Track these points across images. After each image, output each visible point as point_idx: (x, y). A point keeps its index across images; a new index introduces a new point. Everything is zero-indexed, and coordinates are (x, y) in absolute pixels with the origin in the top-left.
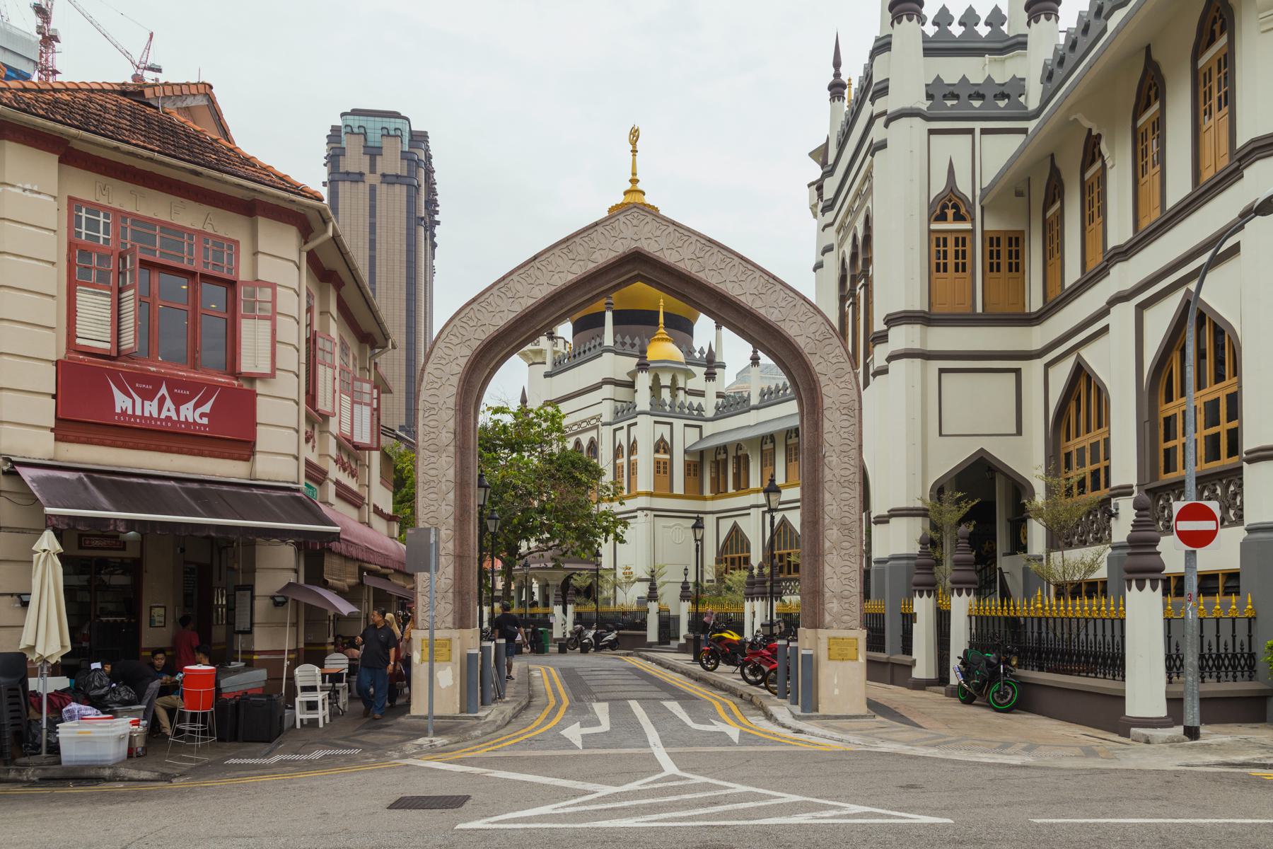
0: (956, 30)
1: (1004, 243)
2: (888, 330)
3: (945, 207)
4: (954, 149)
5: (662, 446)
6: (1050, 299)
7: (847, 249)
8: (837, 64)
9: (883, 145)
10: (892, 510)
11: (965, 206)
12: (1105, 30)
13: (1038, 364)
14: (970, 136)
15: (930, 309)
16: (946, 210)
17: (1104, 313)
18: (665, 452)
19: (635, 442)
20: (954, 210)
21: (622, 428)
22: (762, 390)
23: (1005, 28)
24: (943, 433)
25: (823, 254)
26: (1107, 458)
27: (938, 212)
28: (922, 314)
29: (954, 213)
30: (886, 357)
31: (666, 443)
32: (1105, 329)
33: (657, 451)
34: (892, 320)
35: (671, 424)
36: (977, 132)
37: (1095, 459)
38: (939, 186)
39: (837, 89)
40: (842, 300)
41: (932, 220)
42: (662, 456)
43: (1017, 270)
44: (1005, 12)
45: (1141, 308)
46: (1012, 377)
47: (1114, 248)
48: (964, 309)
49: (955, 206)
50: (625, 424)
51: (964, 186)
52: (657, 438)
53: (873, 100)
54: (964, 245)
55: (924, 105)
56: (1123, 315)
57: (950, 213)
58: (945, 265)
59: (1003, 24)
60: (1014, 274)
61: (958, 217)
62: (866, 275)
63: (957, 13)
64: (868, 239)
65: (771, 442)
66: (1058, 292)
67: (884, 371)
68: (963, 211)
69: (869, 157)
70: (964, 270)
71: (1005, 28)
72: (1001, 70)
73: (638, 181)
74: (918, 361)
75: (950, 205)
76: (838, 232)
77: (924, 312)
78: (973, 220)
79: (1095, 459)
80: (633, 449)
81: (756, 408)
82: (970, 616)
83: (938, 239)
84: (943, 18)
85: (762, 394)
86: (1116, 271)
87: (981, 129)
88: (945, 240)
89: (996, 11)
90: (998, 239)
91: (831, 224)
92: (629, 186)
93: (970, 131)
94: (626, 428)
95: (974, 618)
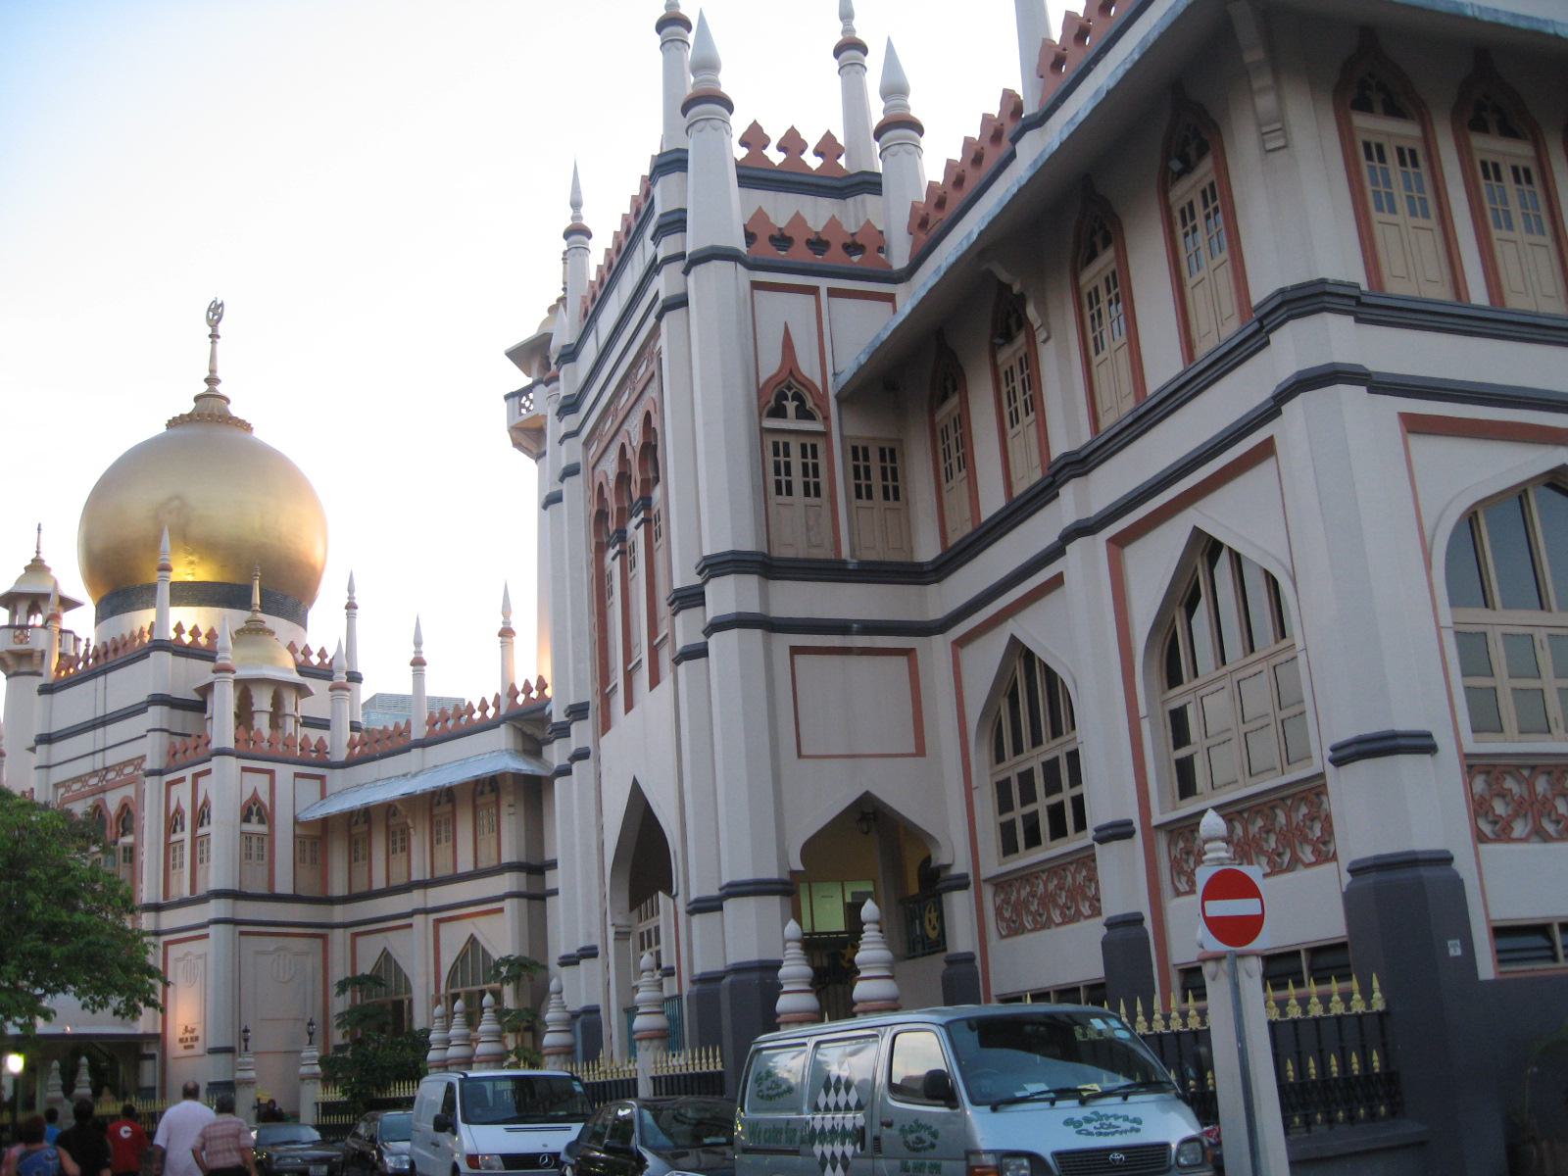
0: (776, 157)
1: (875, 456)
2: (705, 582)
3: (782, 396)
4: (786, 312)
5: (254, 810)
6: (951, 542)
7: (610, 467)
8: (576, 205)
9: (680, 302)
10: (729, 885)
11: (813, 398)
13: (941, 644)
15: (769, 550)
16: (784, 402)
17: (1056, 552)
18: (261, 821)
19: (206, 803)
20: (796, 403)
21: (182, 780)
22: (431, 715)
23: (842, 161)
25: (562, 480)
26: (1076, 779)
27: (773, 402)
28: (760, 559)
29: (797, 408)
32: (1058, 581)
33: (246, 819)
34: (716, 566)
35: (271, 772)
36: (823, 293)
37: (1053, 786)
38: (771, 364)
39: (577, 232)
40: (600, 549)
41: (765, 413)
44: (841, 140)
45: (1120, 542)
47: (1065, 455)
48: (824, 553)
49: (798, 397)
50: (188, 773)
51: (808, 365)
52: (247, 796)
54: (815, 455)
55: (739, 243)
56: (1085, 561)
57: (791, 406)
58: (789, 484)
59: (839, 156)
60: (891, 503)
61: (803, 413)
62: (646, 502)
63: (775, 133)
64: (650, 450)
65: (449, 801)
66: (968, 529)
67: (698, 652)
68: (810, 404)
69: (651, 320)
70: (818, 494)
71: (842, 161)
72: (853, 213)
74: (757, 634)
75: (790, 395)
76: (587, 444)
77: (763, 554)
78: (826, 418)
79: (1053, 786)
80: (201, 816)
81: (422, 744)
83: (776, 445)
84: (755, 138)
85: (432, 722)
86: (1068, 492)
87: (829, 289)
89: (829, 138)
90: (865, 450)
91: (575, 434)
92: (203, 388)
93: (813, 291)
94: (189, 779)
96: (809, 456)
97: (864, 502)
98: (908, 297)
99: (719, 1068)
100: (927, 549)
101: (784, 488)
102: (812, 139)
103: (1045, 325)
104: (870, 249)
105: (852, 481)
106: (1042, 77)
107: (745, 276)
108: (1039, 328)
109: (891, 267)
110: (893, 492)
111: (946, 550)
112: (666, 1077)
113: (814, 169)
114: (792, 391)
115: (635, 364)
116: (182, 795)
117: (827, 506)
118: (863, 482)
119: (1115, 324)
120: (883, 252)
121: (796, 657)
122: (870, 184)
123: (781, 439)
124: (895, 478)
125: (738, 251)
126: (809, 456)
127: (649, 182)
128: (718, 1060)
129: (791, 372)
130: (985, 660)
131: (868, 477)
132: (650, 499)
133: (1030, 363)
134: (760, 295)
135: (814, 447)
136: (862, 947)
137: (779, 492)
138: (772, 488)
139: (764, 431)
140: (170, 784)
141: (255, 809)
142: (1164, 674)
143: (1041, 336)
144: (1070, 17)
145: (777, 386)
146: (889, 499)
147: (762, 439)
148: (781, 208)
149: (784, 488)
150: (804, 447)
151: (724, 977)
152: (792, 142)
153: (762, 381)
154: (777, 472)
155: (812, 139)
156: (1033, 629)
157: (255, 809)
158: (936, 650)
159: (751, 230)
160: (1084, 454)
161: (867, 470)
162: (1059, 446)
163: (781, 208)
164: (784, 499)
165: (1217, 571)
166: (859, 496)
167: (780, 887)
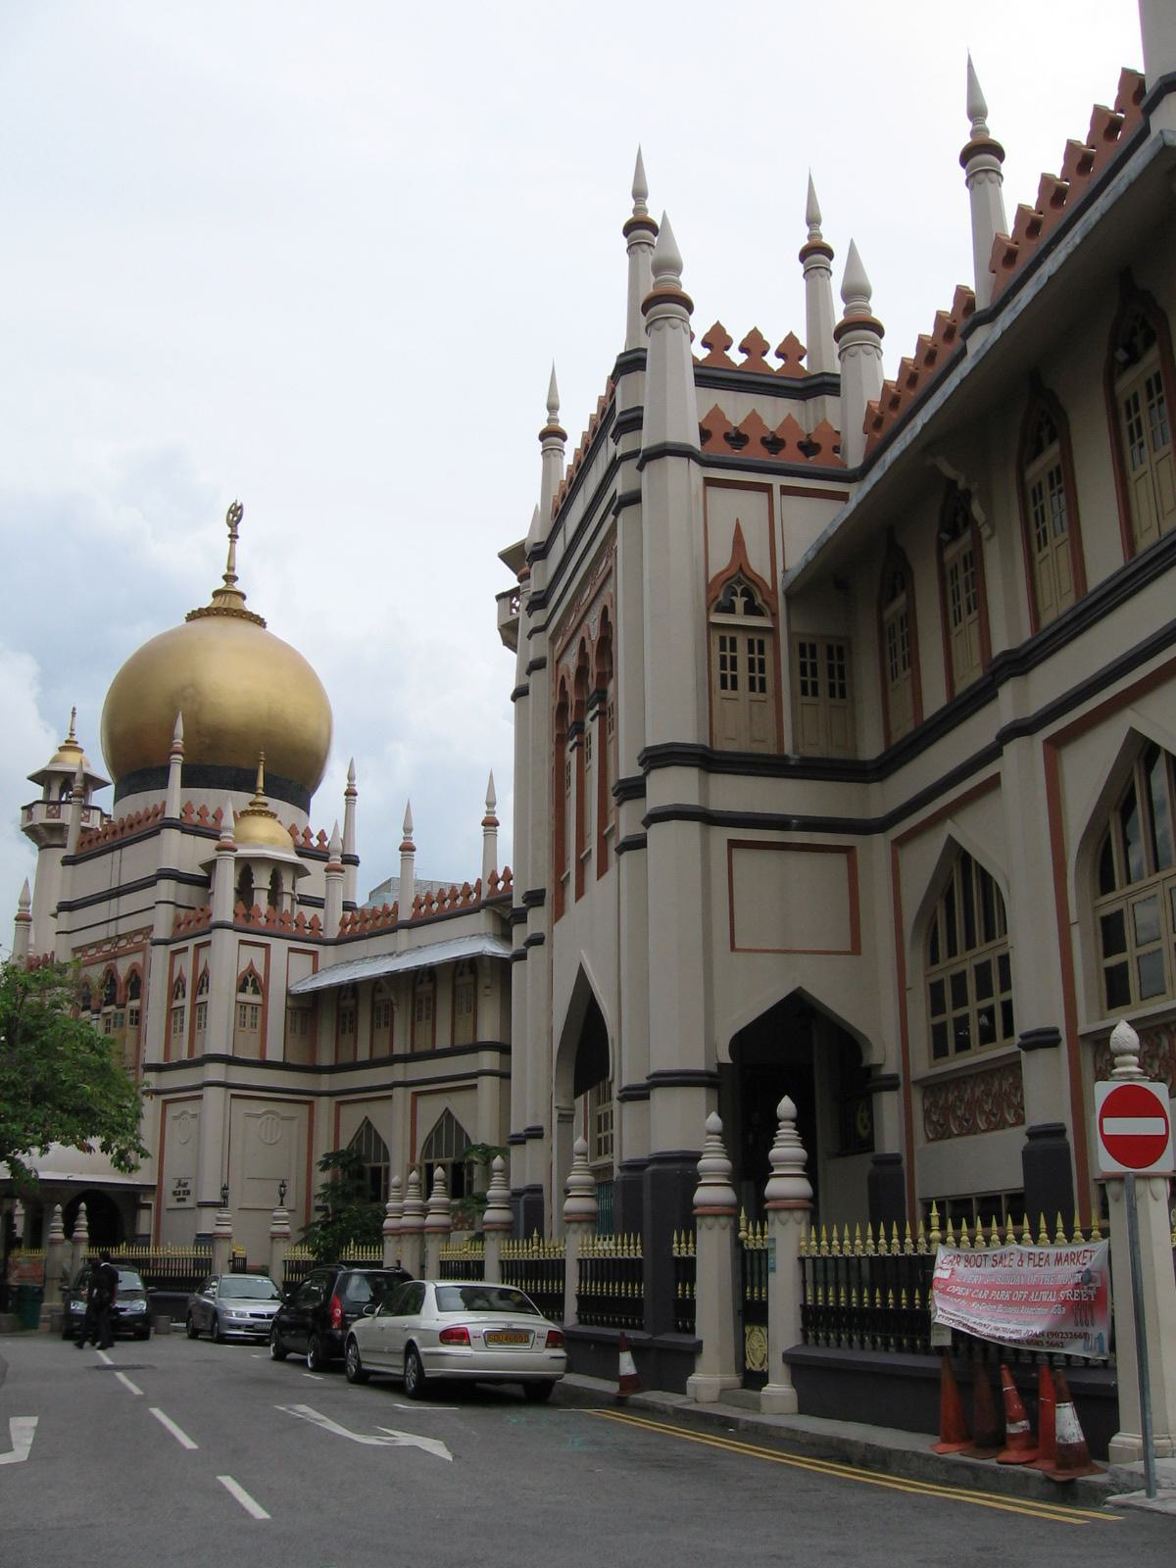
0: (737, 357)
1: (822, 653)
2: (646, 774)
4: (746, 508)
5: (250, 981)
6: (894, 742)
7: (571, 661)
8: (552, 408)
9: (633, 499)
10: (655, 1075)
12: (963, 352)
13: (880, 843)
14: (765, 496)
17: (993, 753)
18: (256, 992)
19: (206, 973)
21: (185, 949)
22: (417, 899)
24: (737, 946)
25: (528, 673)
26: (1006, 985)
28: (700, 751)
29: (745, 603)
30: (642, 818)
31: (256, 978)
33: (242, 989)
34: (658, 758)
35: (267, 946)
36: (776, 491)
37: (984, 991)
38: (721, 559)
39: (552, 435)
40: (560, 741)
41: (712, 609)
42: (249, 997)
43: (843, 695)
44: (803, 342)
45: (1056, 744)
46: (839, 862)
47: (1005, 653)
48: (768, 749)
50: (191, 944)
51: (758, 562)
53: (616, 438)
55: (694, 441)
56: (1021, 763)
58: (734, 679)
59: (801, 358)
61: (752, 609)
62: (601, 695)
63: (738, 334)
64: (606, 643)
65: (430, 980)
66: (910, 727)
67: (637, 843)
68: (759, 601)
69: (611, 517)
70: (763, 689)
71: (804, 363)
73: (235, 579)
74: (694, 828)
76: (553, 639)
77: (704, 747)
78: (774, 615)
79: (984, 991)
80: (202, 983)
82: (802, 1260)
83: (723, 640)
84: (717, 339)
85: (418, 905)
86: (1007, 692)
87: (782, 487)
88: (733, 641)
89: (791, 339)
90: (813, 647)
91: (542, 629)
92: (221, 584)
93: (767, 488)
95: (809, 1263)
96: (756, 651)
97: (809, 699)
98: (857, 492)
99: (639, 1256)
100: (871, 748)
101: (729, 683)
102: (775, 341)
103: (990, 521)
104: (826, 447)
105: (798, 677)
106: (994, 272)
107: (697, 473)
108: (983, 525)
109: (846, 466)
110: (840, 690)
111: (889, 749)
112: (591, 1260)
113: (775, 370)
114: (742, 587)
115: (596, 561)
116: (185, 964)
117: (771, 702)
118: (809, 679)
119: (1057, 520)
120: (838, 453)
121: (734, 850)
122: (825, 386)
123: (728, 635)
124: (842, 676)
125: (691, 447)
126: (756, 651)
127: (614, 378)
128: (638, 1247)
129: (741, 568)
130: (923, 861)
131: (814, 674)
132: (605, 692)
133: (974, 561)
134: (712, 491)
135: (761, 643)
136: (776, 1144)
137: (724, 686)
138: (717, 681)
139: (712, 626)
140: (174, 953)
141: (250, 980)
142: (1097, 876)
143: (986, 532)
144: (1022, 210)
145: (724, 583)
146: (835, 697)
147: (709, 636)
148: (737, 408)
149: (729, 683)
150: (751, 643)
151: (647, 1166)
152: (754, 344)
153: (711, 576)
154: (723, 667)
155: (775, 341)
156: (971, 831)
157: (250, 980)
158: (876, 850)
159: (706, 428)
160: (1023, 653)
161: (814, 666)
162: (1001, 644)
163: (737, 408)
164: (729, 693)
165: (1153, 776)
166: (804, 692)
167: (706, 1079)
